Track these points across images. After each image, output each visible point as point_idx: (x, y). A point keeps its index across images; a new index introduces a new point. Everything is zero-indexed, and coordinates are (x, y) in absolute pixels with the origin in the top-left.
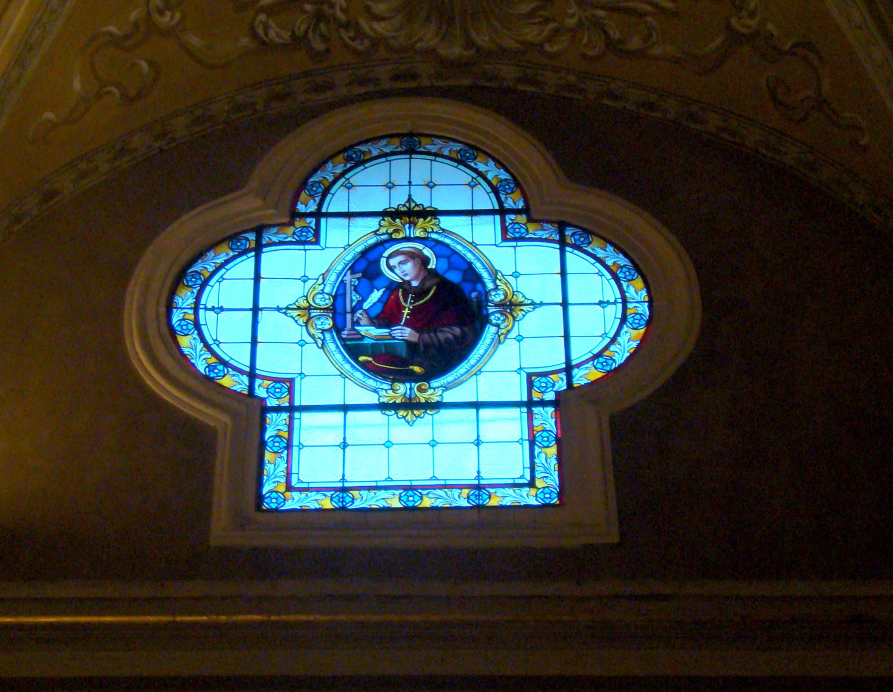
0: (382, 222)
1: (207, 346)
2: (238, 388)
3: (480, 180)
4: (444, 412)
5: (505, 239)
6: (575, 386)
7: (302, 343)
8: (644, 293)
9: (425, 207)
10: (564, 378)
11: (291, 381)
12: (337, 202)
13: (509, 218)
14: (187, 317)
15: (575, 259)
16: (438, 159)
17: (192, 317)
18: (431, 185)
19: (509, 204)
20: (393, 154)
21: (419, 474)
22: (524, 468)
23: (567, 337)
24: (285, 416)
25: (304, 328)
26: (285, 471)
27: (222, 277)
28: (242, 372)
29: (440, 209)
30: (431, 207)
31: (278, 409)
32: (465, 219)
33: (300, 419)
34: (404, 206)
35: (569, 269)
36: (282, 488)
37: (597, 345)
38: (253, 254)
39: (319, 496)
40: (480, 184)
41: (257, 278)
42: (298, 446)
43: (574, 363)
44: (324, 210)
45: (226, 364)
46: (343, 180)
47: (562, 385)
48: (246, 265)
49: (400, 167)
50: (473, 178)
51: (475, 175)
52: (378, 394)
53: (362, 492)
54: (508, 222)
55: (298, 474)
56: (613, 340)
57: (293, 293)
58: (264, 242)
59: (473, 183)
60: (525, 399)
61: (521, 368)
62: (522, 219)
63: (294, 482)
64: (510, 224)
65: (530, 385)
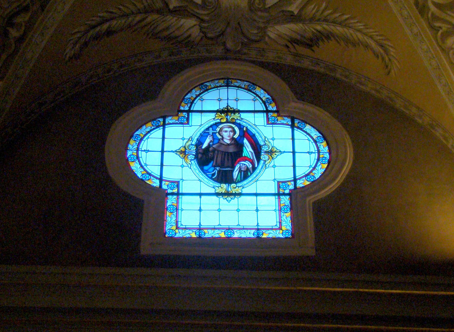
0: (216, 115)
1: (142, 166)
2: (155, 185)
3: (257, 97)
4: (243, 197)
5: (268, 123)
6: (298, 187)
7: (182, 166)
8: (327, 148)
9: (235, 109)
10: (293, 184)
11: (178, 182)
12: (197, 106)
13: (270, 114)
14: (134, 154)
15: (298, 134)
16: (239, 89)
17: (136, 154)
18: (237, 100)
19: (270, 108)
20: (220, 86)
21: (232, 223)
22: (277, 222)
23: (294, 166)
24: (175, 197)
25: (183, 159)
26: (176, 221)
27: (148, 137)
28: (157, 178)
29: (241, 110)
30: (237, 109)
31: (173, 194)
32: (252, 115)
33: (182, 198)
34: (225, 108)
35: (296, 137)
36: (174, 228)
37: (307, 170)
38: (162, 127)
39: (190, 232)
40: (258, 100)
41: (163, 138)
42: (181, 210)
43: (297, 178)
44: (192, 109)
45: (150, 174)
46: (199, 98)
47: (292, 187)
48: (158, 133)
49: (223, 92)
50: (254, 97)
51: (255, 96)
52: (215, 189)
53: (209, 230)
54: (270, 116)
55: (181, 222)
56: (314, 168)
57: (178, 145)
58: (167, 122)
59: (255, 99)
60: (277, 192)
61: (275, 179)
62: (275, 115)
63: (179, 225)
64: (270, 117)
65: (279, 187)
